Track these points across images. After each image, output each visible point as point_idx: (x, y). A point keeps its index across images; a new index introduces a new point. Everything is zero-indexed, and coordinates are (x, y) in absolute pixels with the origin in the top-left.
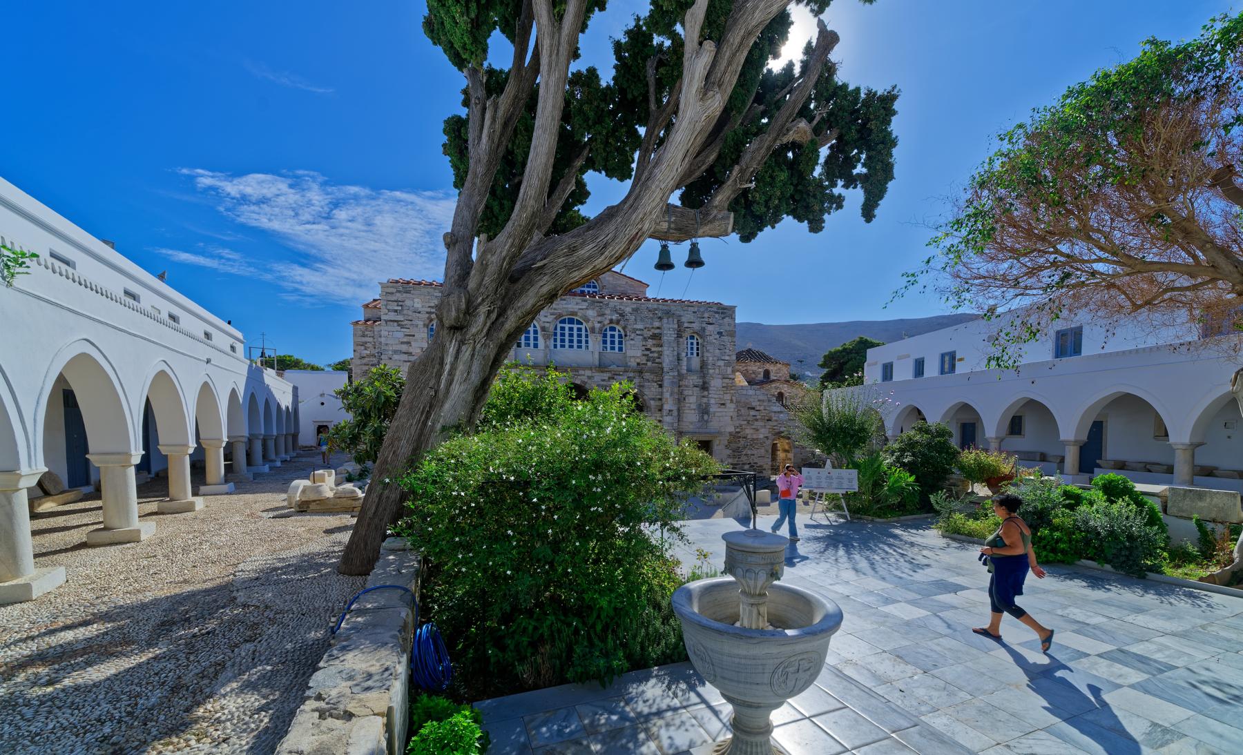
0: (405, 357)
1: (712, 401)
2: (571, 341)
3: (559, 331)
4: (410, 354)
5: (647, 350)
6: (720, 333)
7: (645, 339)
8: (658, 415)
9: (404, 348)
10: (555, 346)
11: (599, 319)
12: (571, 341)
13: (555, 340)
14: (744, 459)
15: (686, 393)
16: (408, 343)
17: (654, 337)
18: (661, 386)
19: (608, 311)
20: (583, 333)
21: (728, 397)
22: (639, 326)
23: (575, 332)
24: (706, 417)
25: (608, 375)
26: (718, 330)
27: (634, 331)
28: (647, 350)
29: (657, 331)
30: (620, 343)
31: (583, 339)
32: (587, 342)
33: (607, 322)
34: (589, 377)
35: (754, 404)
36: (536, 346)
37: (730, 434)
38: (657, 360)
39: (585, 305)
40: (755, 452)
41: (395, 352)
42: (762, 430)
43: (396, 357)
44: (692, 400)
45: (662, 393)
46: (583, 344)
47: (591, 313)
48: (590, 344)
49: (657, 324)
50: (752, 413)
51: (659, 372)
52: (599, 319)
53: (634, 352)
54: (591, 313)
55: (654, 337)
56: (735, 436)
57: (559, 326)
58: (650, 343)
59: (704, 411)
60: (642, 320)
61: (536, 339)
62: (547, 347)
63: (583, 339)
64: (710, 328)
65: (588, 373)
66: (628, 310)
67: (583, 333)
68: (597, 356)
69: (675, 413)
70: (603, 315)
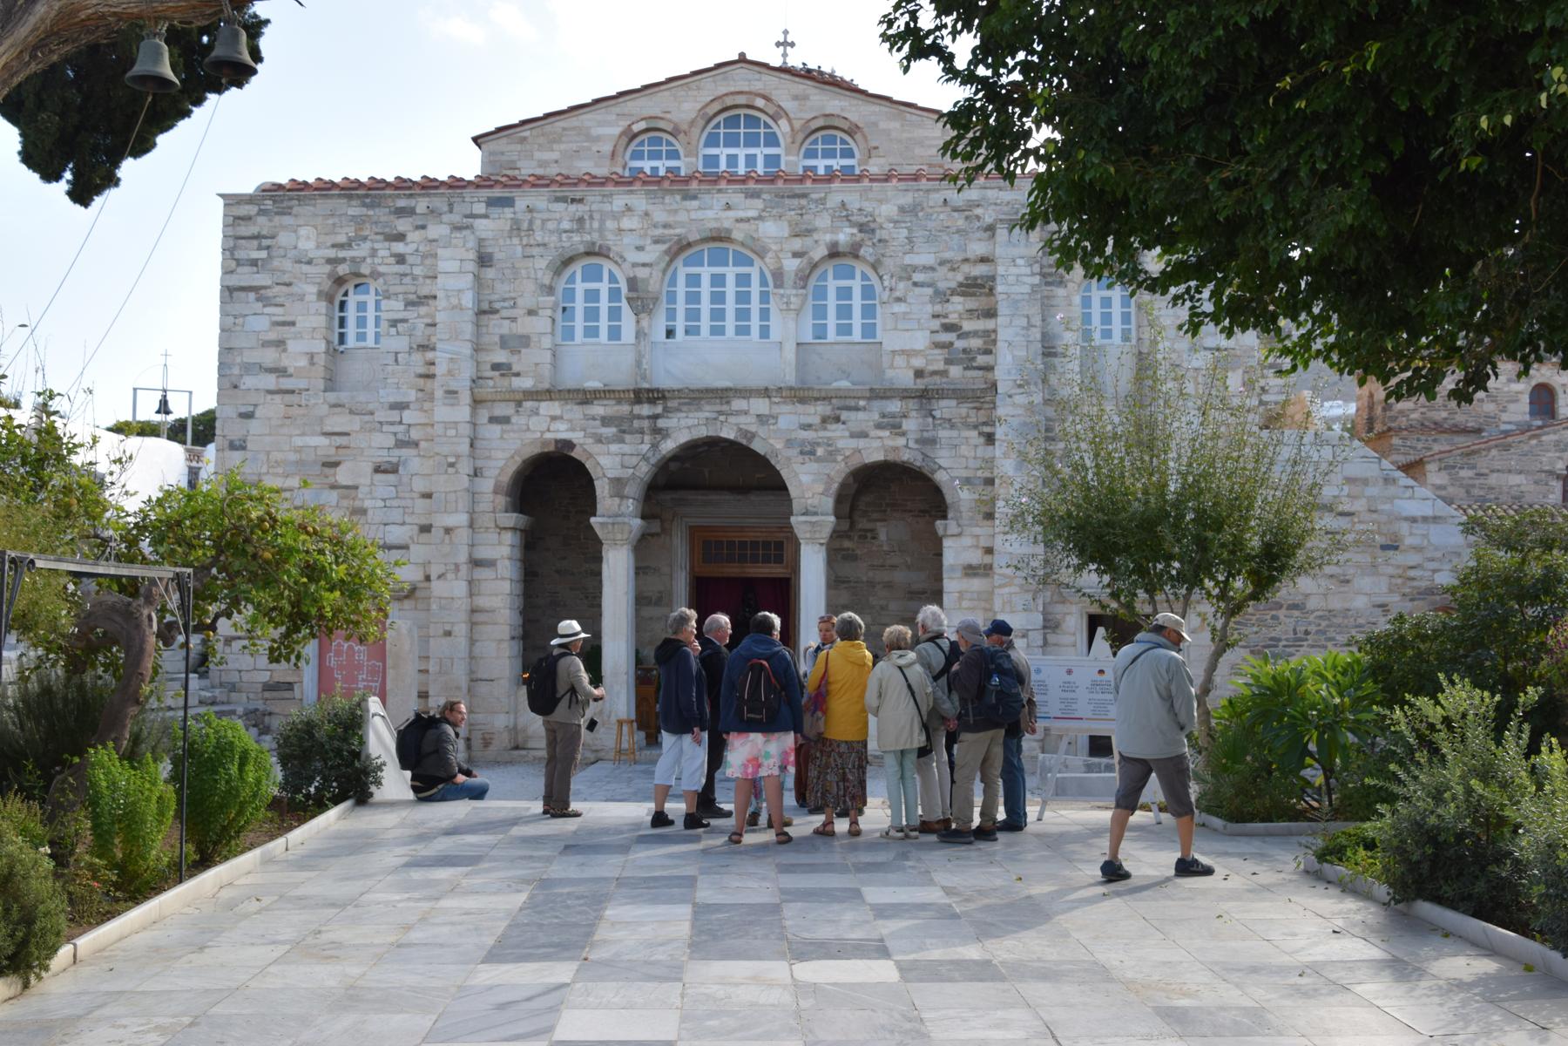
0: (270, 381)
2: (718, 315)
3: (681, 289)
4: (281, 372)
5: (948, 328)
7: (942, 296)
8: (982, 530)
9: (269, 357)
10: (670, 333)
11: (797, 244)
12: (718, 315)
13: (671, 314)
16: (280, 344)
17: (971, 287)
18: (990, 439)
19: (823, 221)
20: (755, 289)
22: (924, 258)
23: (730, 289)
25: (822, 409)
27: (907, 272)
28: (948, 328)
29: (980, 270)
30: (869, 311)
31: (755, 306)
32: (765, 314)
33: (819, 252)
34: (762, 419)
36: (615, 333)
38: (977, 359)
39: (752, 208)
41: (248, 368)
42: (1364, 583)
43: (249, 382)
45: (990, 462)
46: (755, 323)
47: (772, 230)
48: (775, 322)
49: (978, 248)
51: (983, 396)
52: (797, 244)
53: (907, 338)
54: (772, 230)
55: (971, 287)
57: (682, 272)
58: (958, 304)
60: (931, 239)
61: (615, 314)
62: (640, 334)
63: (755, 306)
65: (760, 406)
66: (888, 210)
67: (755, 289)
68: (790, 353)
70: (808, 232)
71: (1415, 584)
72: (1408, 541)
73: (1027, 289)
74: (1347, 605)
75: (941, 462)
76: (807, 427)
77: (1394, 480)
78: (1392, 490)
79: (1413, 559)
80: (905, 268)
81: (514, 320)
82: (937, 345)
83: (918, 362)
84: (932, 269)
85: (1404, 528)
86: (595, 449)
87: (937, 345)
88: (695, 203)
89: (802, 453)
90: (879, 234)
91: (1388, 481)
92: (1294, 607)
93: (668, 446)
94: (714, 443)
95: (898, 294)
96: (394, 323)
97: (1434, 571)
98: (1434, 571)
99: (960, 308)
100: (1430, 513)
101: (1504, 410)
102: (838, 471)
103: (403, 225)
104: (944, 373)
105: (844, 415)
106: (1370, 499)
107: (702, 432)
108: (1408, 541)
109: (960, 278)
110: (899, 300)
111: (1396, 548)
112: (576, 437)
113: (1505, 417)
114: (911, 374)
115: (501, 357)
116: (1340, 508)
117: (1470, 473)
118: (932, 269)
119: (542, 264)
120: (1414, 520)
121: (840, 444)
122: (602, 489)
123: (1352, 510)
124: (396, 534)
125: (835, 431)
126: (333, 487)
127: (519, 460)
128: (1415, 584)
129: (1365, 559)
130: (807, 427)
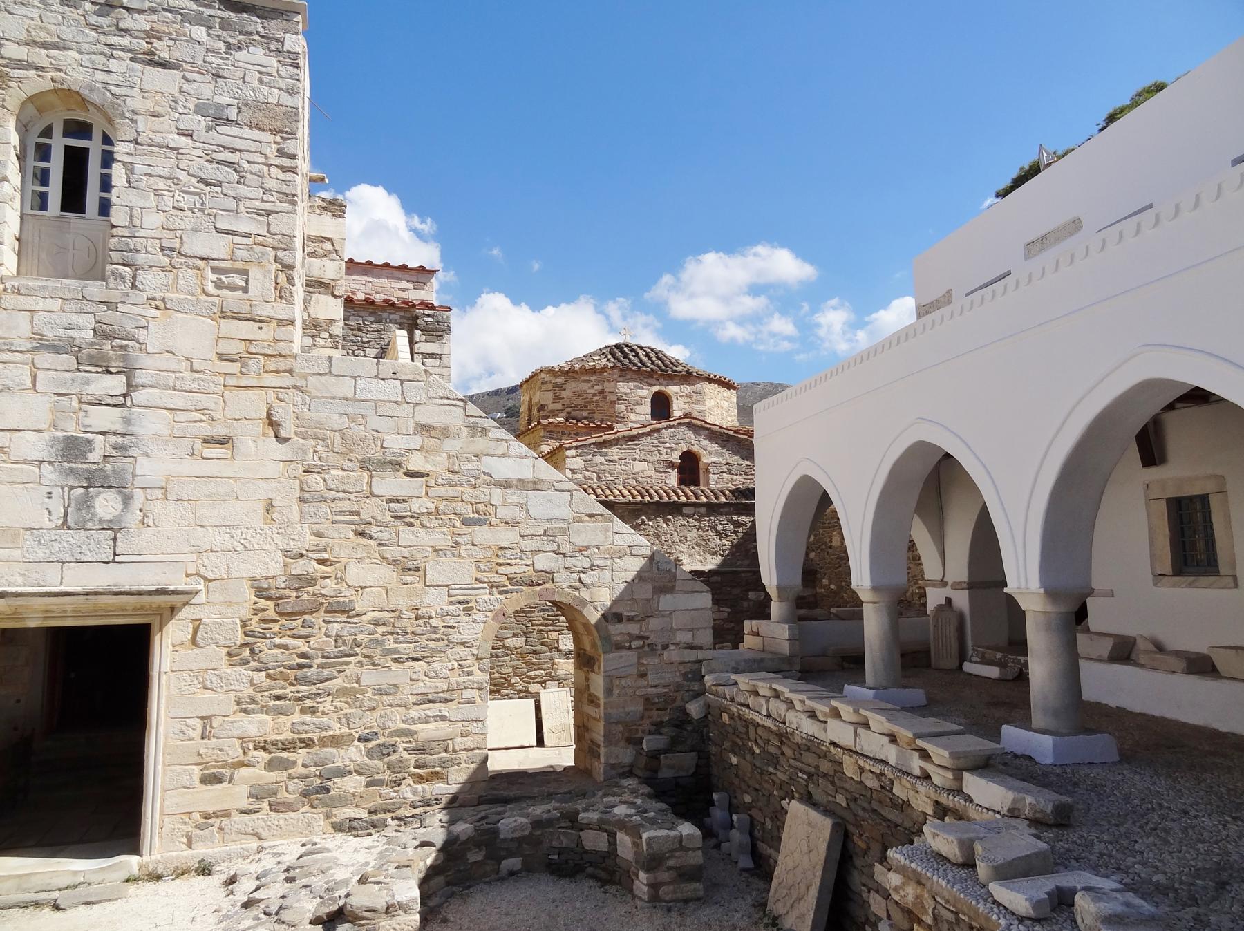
1: (150, 424)
24: (106, 505)
35: (394, 443)
40: (396, 674)
50: (390, 484)
56: (289, 603)
64: (155, 78)
71: (507, 570)
72: (502, 513)
74: (416, 602)
77: (484, 430)
78: (480, 444)
79: (507, 536)
85: (497, 495)
91: (477, 431)
100: (528, 475)
101: (632, 411)
106: (453, 456)
108: (502, 513)
113: (633, 417)
116: (411, 468)
117: (602, 460)
120: (507, 485)
123: (428, 467)
128: (507, 570)
129: (441, 539)
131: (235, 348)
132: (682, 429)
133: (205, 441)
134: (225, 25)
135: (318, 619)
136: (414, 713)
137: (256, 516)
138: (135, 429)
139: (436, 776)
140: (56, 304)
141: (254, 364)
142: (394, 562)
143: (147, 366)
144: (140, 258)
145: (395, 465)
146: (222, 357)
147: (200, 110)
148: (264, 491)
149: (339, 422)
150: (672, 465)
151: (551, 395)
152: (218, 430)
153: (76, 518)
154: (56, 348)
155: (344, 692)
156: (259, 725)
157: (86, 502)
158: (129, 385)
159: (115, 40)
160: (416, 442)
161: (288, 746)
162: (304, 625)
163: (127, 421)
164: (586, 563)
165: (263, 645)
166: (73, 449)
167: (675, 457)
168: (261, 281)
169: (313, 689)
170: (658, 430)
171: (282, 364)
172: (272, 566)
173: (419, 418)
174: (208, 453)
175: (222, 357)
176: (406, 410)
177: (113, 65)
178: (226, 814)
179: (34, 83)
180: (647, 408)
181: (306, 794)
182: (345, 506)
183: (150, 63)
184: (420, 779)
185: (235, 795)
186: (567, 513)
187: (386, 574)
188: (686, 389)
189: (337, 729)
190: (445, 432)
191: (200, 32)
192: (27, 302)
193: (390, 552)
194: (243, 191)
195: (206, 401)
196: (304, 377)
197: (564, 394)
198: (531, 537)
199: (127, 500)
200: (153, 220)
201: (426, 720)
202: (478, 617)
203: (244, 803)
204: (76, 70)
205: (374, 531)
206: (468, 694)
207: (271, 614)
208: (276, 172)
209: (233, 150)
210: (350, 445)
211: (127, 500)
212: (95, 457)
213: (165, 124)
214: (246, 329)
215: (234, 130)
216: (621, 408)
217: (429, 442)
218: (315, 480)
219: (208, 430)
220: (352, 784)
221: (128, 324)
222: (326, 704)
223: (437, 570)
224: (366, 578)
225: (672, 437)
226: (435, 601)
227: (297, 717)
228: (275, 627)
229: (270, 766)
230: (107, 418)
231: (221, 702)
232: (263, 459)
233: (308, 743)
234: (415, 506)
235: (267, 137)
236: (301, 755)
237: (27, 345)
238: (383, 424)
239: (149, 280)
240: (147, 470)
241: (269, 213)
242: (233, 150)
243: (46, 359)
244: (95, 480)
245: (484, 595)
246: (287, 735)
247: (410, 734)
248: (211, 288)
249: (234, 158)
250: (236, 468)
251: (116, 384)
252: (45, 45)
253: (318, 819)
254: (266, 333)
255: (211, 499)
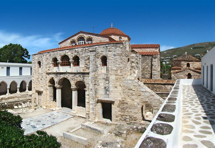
1: (111, 85)
5: (86, 64)
6: (115, 55)
7: (86, 60)
14: (126, 113)
15: (99, 81)
21: (118, 83)
24: (108, 93)
26: (114, 53)
35: (131, 87)
37: (120, 101)
40: (132, 110)
42: (136, 100)
44: (102, 84)
50: (131, 91)
56: (122, 102)
59: (107, 89)
64: (110, 53)
69: (93, 90)
71: (143, 101)
73: (93, 59)
75: (85, 81)
76: (72, 76)
79: (143, 97)
80: (81, 57)
81: (49, 65)
82: (85, 66)
83: (83, 69)
84: (84, 57)
85: (142, 93)
86: (55, 78)
87: (85, 66)
88: (63, 51)
89: (72, 80)
90: (79, 53)
92: (127, 103)
93: (61, 78)
94: (64, 78)
95: (81, 60)
96: (42, 65)
97: (146, 99)
98: (146, 99)
99: (87, 62)
102: (76, 81)
103: (42, 56)
104: (86, 70)
105: (76, 75)
107: (63, 77)
108: (142, 95)
109: (87, 58)
110: (81, 61)
111: (140, 96)
112: (54, 77)
113: (184, 67)
114: (82, 70)
115: (49, 69)
116: (133, 90)
117: (177, 75)
118: (84, 57)
119: (51, 59)
120: (143, 92)
121: (76, 79)
122: (55, 82)
124: (42, 86)
125: (75, 77)
126: (38, 81)
127: (50, 79)
128: (143, 101)
129: (136, 97)
130: (72, 76)
131: (117, 78)
132: (188, 70)
133: (115, 87)
134: (115, 46)
135: (125, 104)
136: (133, 114)
137: (119, 95)
138: (109, 86)
139: (136, 121)
140: (104, 75)
141: (119, 79)
142: (131, 99)
143: (110, 80)
144: (109, 70)
145: (131, 90)
146: (116, 79)
147: (113, 55)
148: (120, 92)
149: (126, 85)
150: (187, 75)
151: (174, 63)
152: (116, 86)
153: (106, 93)
154: (103, 79)
155: (127, 111)
156: (120, 113)
157: (106, 92)
158: (109, 82)
159: (107, 50)
160: (133, 87)
161: (122, 115)
162: (124, 105)
163: (109, 85)
164: (151, 100)
165: (120, 106)
166: (105, 88)
167: (187, 74)
168: (119, 71)
169: (124, 111)
170: (185, 70)
171: (121, 79)
172: (121, 99)
173: (134, 85)
174: (115, 88)
175: (116, 79)
176: (132, 84)
177: (107, 52)
178: (118, 120)
179: (102, 55)
180: (186, 65)
181: (124, 120)
182: (127, 94)
183: (109, 51)
184: (134, 120)
185: (118, 119)
186: (149, 95)
187: (130, 100)
188: (192, 62)
189: (127, 115)
190: (136, 86)
191: (113, 47)
192: (102, 75)
193: (131, 98)
194: (117, 62)
195: (115, 83)
196: (123, 81)
197: (176, 63)
198: (145, 97)
199: (109, 92)
200: (110, 66)
201: (135, 115)
202: (140, 105)
203: (119, 120)
204: (104, 54)
205: (129, 96)
206: (139, 113)
207: (121, 103)
208: (120, 60)
209: (116, 59)
210: (127, 87)
211: (109, 92)
212: (107, 88)
213: (111, 57)
214: (118, 76)
215: (116, 57)
216: (182, 66)
217: (135, 87)
218: (124, 91)
219: (115, 86)
220: (128, 120)
221: (108, 76)
222: (126, 112)
223: (136, 100)
224: (128, 100)
225: (187, 71)
226: (136, 103)
227: (123, 113)
228: (121, 105)
229: (121, 117)
230: (107, 85)
231: (117, 110)
232: (120, 88)
233: (124, 115)
234: (133, 94)
235: (119, 57)
236: (123, 116)
237: (102, 79)
238: (130, 85)
239: (110, 72)
240: (111, 89)
241: (119, 64)
242: (116, 59)
243: (103, 80)
244: (107, 90)
245: (140, 103)
246: (122, 114)
247: (133, 116)
248: (115, 73)
249: (116, 59)
250: (117, 90)
251: (108, 82)
252: (102, 52)
253: (125, 122)
254: (119, 77)
255: (115, 92)
